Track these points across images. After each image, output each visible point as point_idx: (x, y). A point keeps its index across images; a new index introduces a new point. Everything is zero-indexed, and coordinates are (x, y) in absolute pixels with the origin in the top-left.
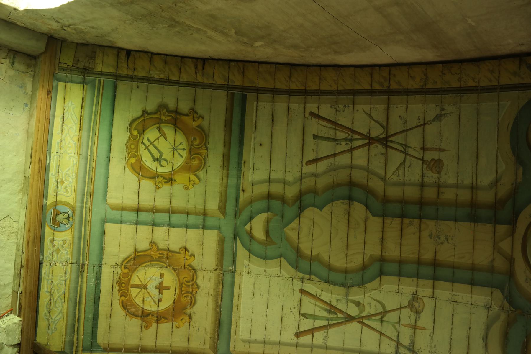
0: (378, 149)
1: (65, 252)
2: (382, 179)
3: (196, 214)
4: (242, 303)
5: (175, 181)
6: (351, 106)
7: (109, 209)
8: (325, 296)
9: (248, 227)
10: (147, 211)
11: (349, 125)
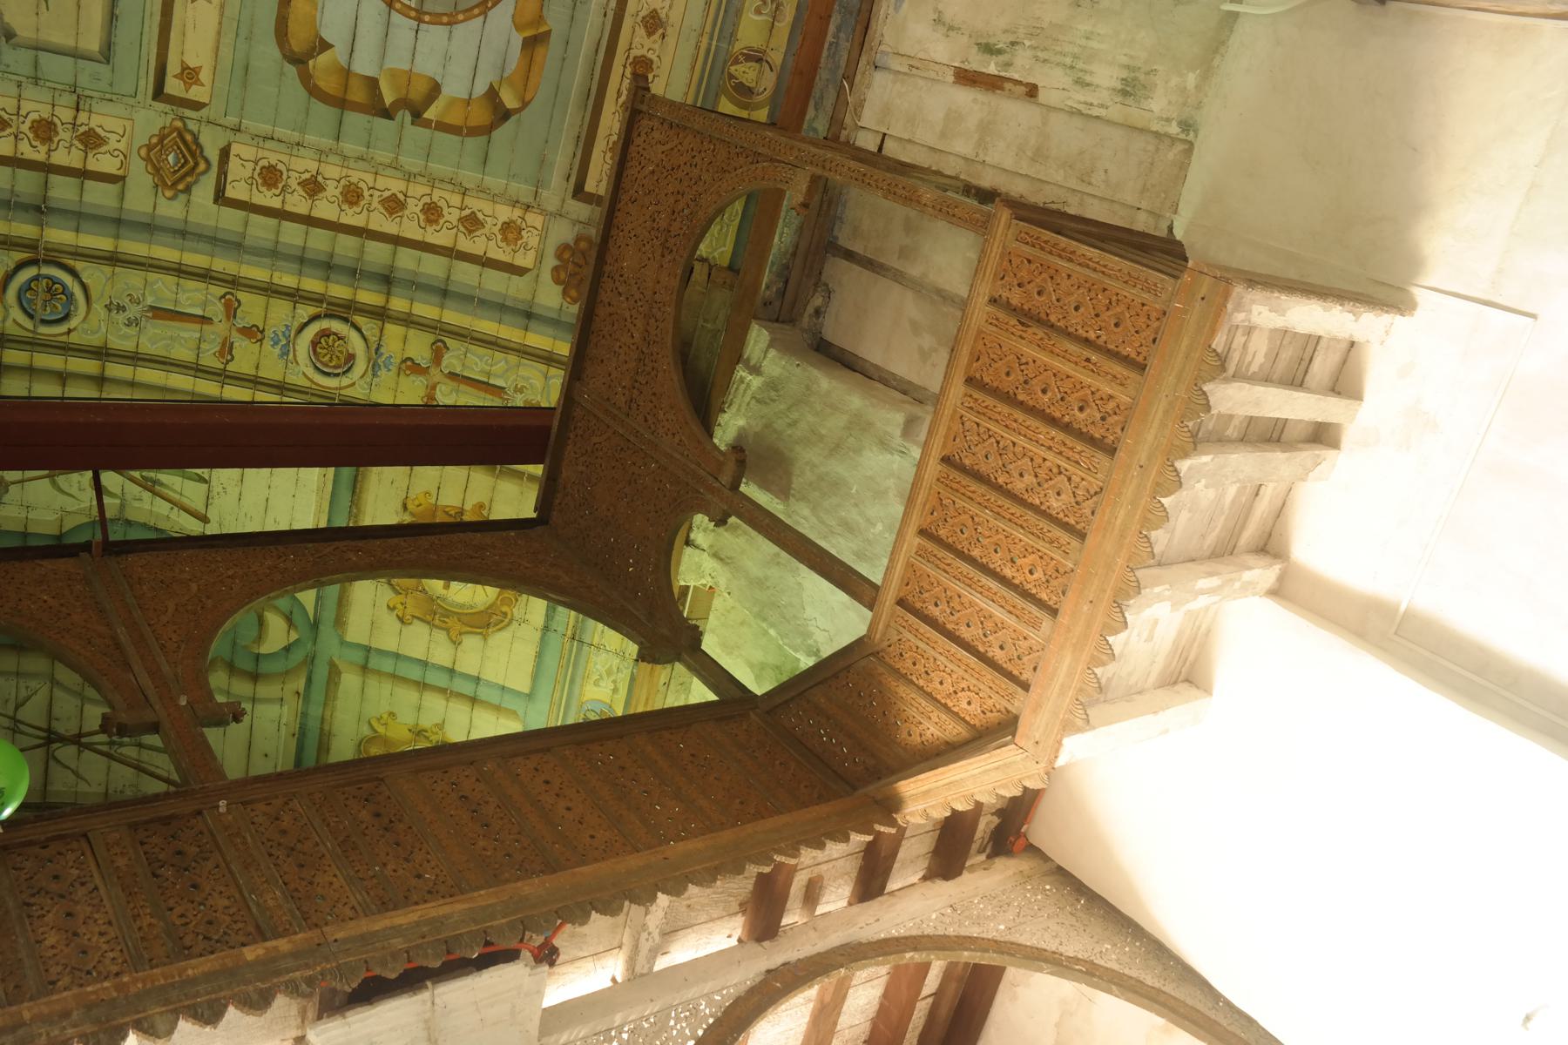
0: (65, 727)
1: (598, 667)
2: (58, 683)
3: (379, 673)
4: (312, 515)
5: (410, 730)
6: (110, 791)
7: (520, 712)
8: (162, 507)
9: (294, 636)
10: (460, 695)
11: (115, 765)
